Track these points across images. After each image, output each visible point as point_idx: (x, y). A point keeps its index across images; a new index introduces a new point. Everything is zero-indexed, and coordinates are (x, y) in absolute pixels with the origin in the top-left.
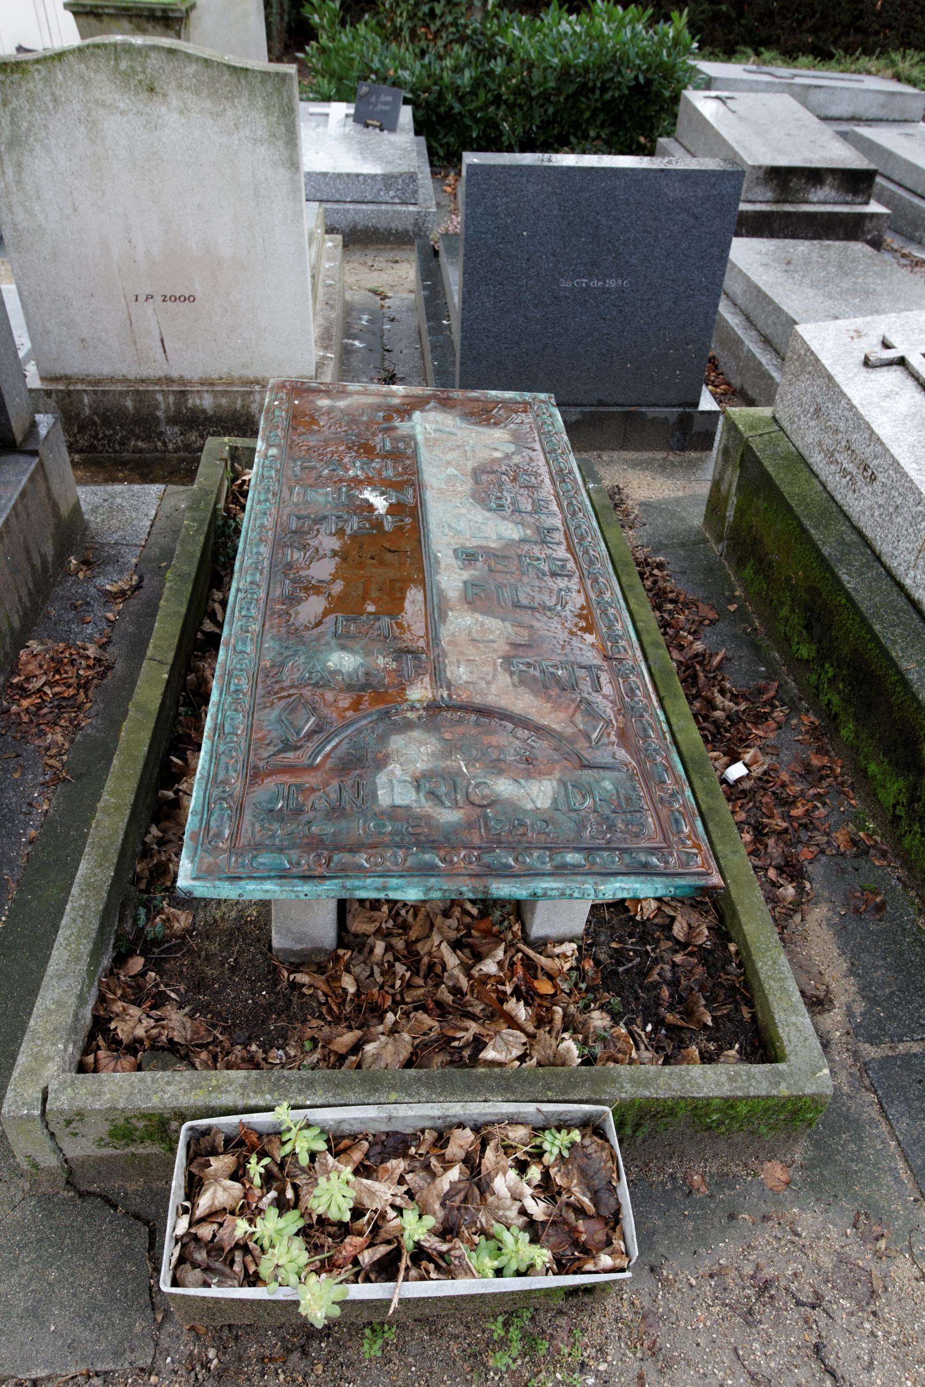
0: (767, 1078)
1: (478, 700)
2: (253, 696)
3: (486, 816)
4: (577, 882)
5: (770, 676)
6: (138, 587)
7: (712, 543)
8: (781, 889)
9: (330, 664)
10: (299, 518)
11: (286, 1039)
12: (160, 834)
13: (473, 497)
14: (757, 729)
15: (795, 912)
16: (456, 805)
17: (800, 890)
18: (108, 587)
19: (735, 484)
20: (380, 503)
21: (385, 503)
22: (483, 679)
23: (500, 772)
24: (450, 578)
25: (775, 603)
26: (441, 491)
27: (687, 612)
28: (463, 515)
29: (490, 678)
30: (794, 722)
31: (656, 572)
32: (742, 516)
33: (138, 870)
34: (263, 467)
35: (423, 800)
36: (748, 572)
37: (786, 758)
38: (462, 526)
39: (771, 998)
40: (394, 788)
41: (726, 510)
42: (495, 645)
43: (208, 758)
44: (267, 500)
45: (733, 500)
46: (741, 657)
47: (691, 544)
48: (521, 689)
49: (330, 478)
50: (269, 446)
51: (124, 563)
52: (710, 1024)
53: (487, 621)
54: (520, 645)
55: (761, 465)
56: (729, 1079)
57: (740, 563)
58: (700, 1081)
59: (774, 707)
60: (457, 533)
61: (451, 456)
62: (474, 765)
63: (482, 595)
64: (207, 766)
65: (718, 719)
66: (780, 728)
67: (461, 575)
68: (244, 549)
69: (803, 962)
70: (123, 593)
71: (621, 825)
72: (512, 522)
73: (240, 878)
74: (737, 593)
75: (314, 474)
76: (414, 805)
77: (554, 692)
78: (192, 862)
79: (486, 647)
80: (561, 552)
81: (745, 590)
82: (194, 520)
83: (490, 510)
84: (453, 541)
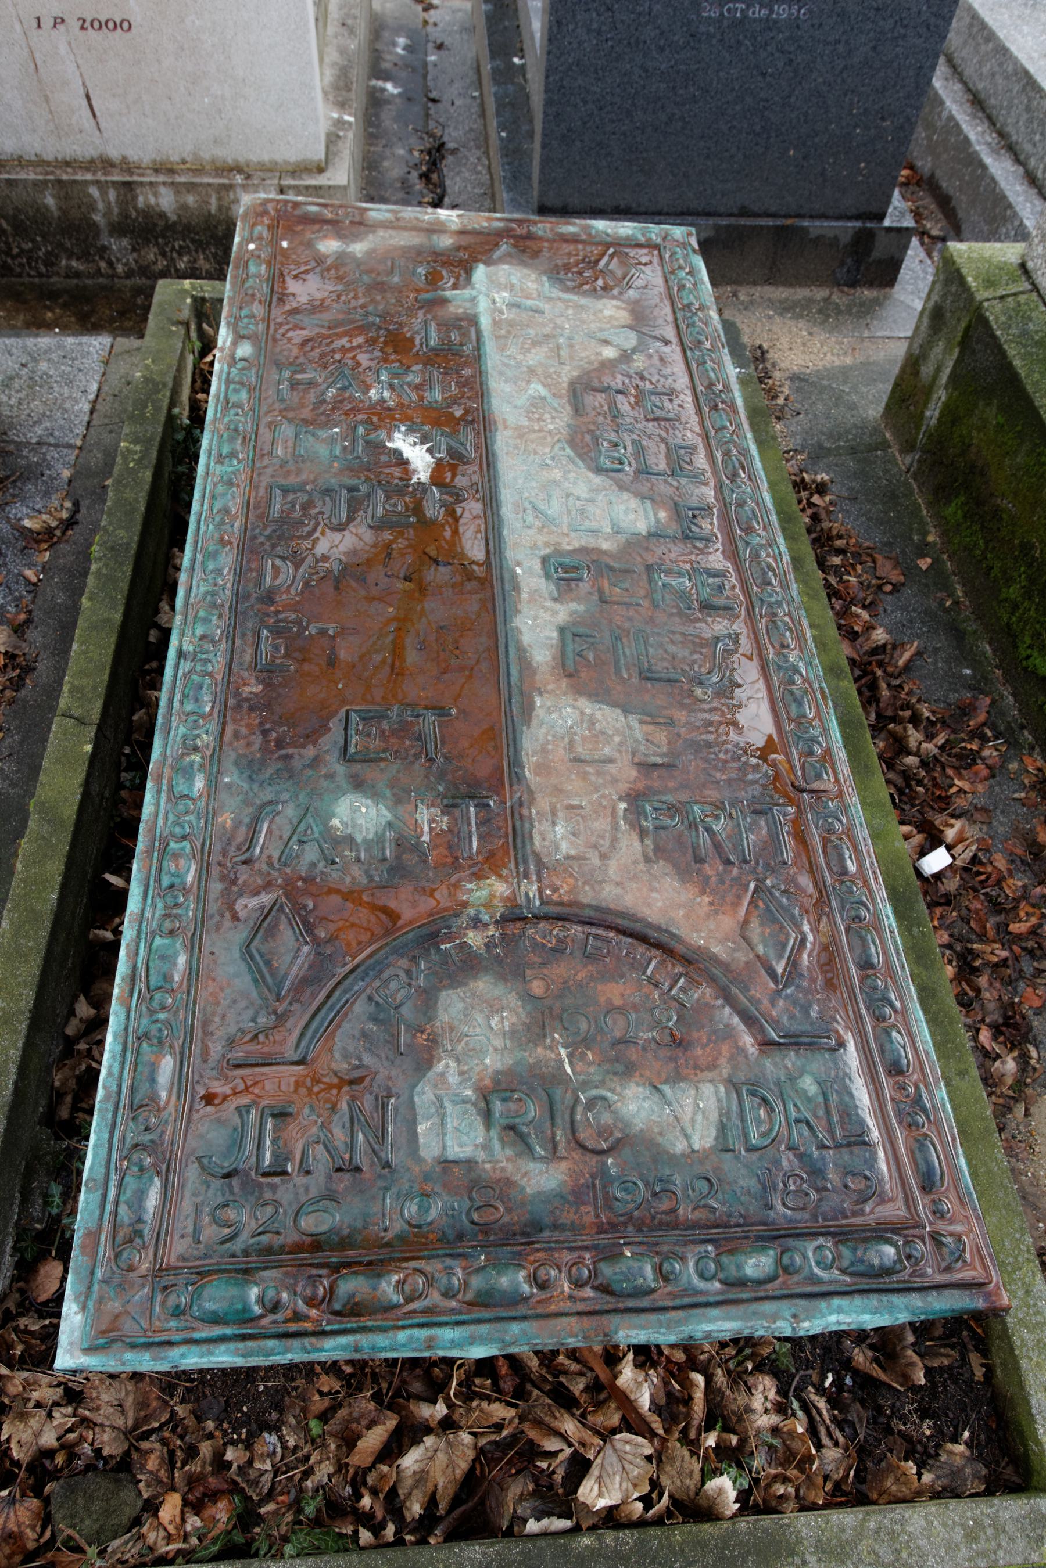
0: (1023, 1530)
1: (587, 896)
2: (202, 899)
3: (607, 1180)
4: (764, 1316)
5: (980, 685)
6: (70, 523)
7: (894, 450)
8: (997, 1063)
9: (335, 822)
10: (285, 491)
11: (281, 1412)
12: (92, 1012)
13: (572, 443)
14: (961, 777)
15: (1016, 1100)
16: (554, 1154)
17: (1023, 1060)
18: (27, 523)
19: (947, 371)
20: (420, 459)
21: (428, 458)
22: (595, 847)
23: (628, 1071)
24: (538, 623)
25: (995, 572)
26: (521, 433)
27: (859, 567)
28: (556, 483)
29: (606, 843)
30: (1013, 766)
31: (816, 499)
32: (953, 423)
33: (57, 1084)
34: (228, 382)
35: (497, 1145)
36: (953, 510)
37: (1001, 830)
38: (555, 508)
39: (1024, 1364)
40: (449, 1129)
41: (925, 405)
42: (612, 769)
43: (119, 1048)
44: (233, 455)
45: (941, 395)
46: (936, 650)
47: (864, 449)
48: (660, 867)
49: (338, 403)
50: (239, 337)
51: (52, 479)
52: (923, 1382)
53: (598, 715)
54: (655, 765)
55: (1003, 354)
56: (966, 1535)
57: (940, 494)
58: (923, 1542)
59: (984, 739)
60: (547, 522)
61: (536, 357)
62: (583, 1055)
63: (591, 657)
64: (116, 1070)
65: (909, 767)
66: (993, 776)
67: (555, 613)
68: (193, 561)
69: (1028, 1189)
70: (49, 531)
71: (833, 1176)
72: (636, 494)
73: (170, 1344)
74: (931, 538)
75: (312, 396)
76: (481, 1156)
77: (712, 869)
78: (84, 1308)
79: (598, 774)
80: (717, 560)
81: (944, 534)
82: (136, 441)
83: (599, 470)
84: (541, 539)
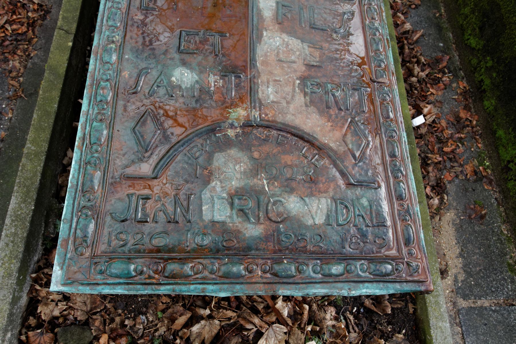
1: (280, 119)
3: (279, 233)
4: (337, 288)
5: (445, 51)
8: (431, 200)
9: (173, 79)
11: (147, 308)
14: (433, 88)
15: (436, 214)
17: (442, 200)
22: (285, 98)
23: (292, 191)
29: (289, 97)
30: (454, 85)
33: (60, 182)
35: (235, 216)
37: (446, 110)
39: (429, 309)
42: (295, 66)
43: (77, 167)
46: (430, 34)
48: (312, 109)
52: (390, 312)
54: (313, 66)
59: (444, 73)
62: (273, 183)
63: (289, 16)
64: (76, 176)
65: (413, 82)
66: (446, 89)
71: (370, 237)
73: (98, 284)
76: (228, 220)
77: (333, 111)
78: (62, 268)
79: (289, 67)
